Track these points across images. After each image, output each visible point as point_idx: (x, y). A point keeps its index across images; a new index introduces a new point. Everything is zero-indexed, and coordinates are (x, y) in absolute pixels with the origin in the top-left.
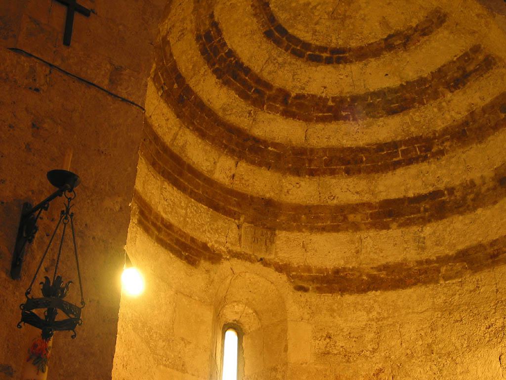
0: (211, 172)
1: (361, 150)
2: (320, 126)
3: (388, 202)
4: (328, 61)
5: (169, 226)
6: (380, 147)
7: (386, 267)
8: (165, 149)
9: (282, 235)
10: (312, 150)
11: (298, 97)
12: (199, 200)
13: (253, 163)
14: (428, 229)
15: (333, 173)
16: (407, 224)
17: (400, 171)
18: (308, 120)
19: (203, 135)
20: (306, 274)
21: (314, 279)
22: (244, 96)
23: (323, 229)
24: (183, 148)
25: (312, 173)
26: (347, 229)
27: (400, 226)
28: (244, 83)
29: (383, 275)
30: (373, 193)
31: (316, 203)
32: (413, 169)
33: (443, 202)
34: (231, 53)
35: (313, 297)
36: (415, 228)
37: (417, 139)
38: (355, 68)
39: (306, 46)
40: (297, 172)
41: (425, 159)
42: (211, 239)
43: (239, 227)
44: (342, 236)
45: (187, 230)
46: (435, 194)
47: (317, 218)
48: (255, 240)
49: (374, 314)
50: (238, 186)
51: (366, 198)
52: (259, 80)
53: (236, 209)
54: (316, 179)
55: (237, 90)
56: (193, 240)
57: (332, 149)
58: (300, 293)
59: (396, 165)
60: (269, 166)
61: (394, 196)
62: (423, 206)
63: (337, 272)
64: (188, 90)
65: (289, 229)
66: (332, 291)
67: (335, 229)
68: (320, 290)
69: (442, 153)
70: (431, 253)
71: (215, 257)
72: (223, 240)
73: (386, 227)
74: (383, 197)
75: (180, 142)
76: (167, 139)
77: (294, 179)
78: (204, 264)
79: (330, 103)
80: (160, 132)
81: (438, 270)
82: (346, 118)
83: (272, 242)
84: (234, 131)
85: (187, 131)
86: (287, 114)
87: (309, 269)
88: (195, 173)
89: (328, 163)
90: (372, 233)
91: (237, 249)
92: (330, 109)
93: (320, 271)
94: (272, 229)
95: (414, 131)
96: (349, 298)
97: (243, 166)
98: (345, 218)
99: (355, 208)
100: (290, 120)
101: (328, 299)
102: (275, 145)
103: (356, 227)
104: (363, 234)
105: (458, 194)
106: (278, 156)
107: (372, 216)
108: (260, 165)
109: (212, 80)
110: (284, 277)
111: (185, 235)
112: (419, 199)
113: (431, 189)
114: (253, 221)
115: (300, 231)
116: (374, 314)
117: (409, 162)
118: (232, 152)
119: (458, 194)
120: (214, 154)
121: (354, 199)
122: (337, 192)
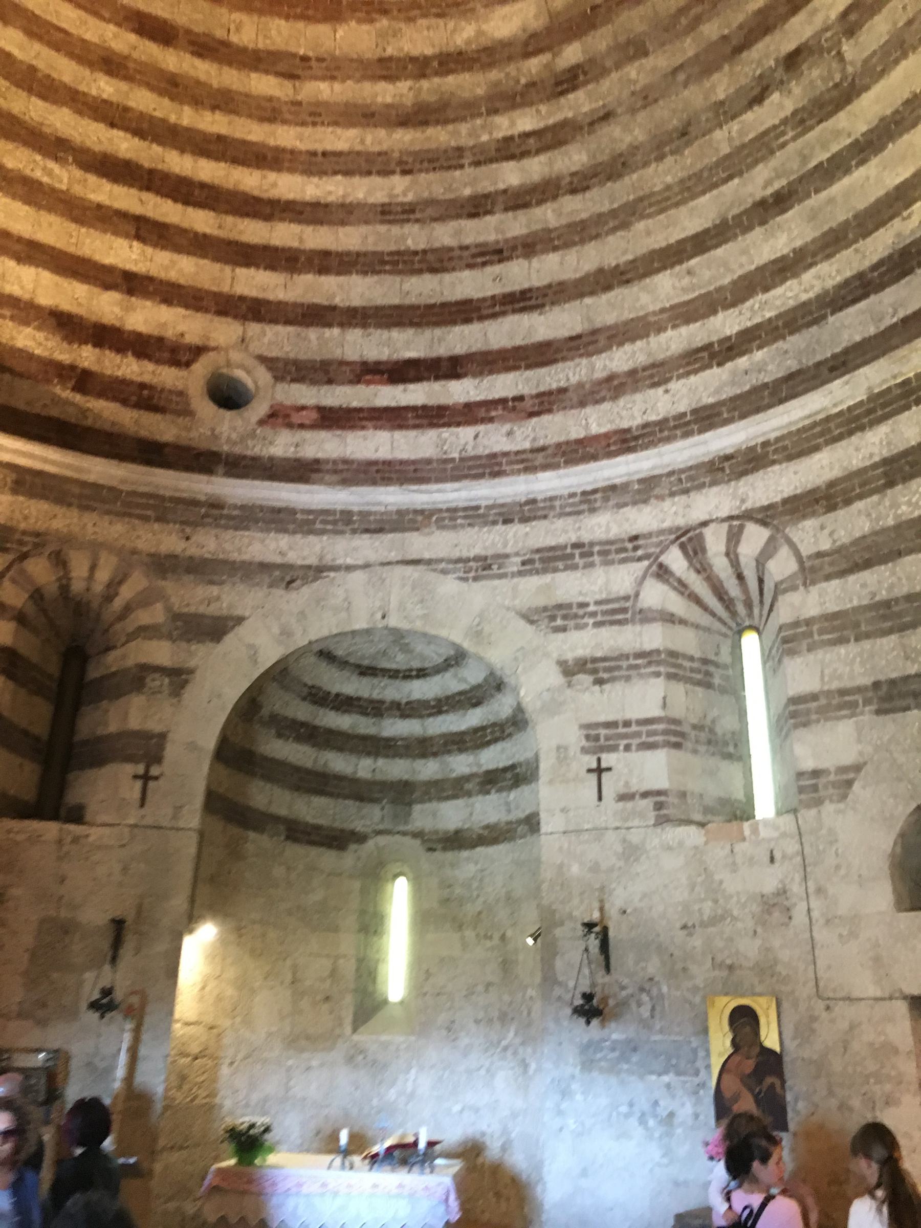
0: (355, 772)
1: (463, 733)
2: (431, 719)
3: (488, 772)
4: (418, 677)
5: (317, 828)
6: (476, 730)
7: (487, 827)
8: (308, 772)
9: (417, 808)
10: (431, 738)
11: (407, 703)
12: (346, 797)
13: (387, 756)
14: (513, 795)
15: (449, 752)
16: (500, 790)
17: (492, 747)
18: (421, 717)
19: (340, 749)
20: (434, 837)
21: (439, 841)
22: (364, 713)
23: (448, 798)
24: (325, 764)
25: (435, 755)
26: (463, 796)
27: (497, 791)
28: (360, 706)
29: (486, 833)
30: (480, 766)
31: (439, 776)
32: (499, 746)
33: (518, 774)
34: (337, 695)
35: (438, 855)
36: (504, 794)
37: (494, 725)
38: (437, 679)
39: (397, 672)
40: (424, 755)
41: (504, 739)
42: (359, 826)
43: (383, 809)
44: (460, 802)
45: (337, 825)
46: (513, 767)
47: (443, 790)
48: (395, 817)
49: (479, 866)
50: (379, 777)
51: (475, 769)
52: (372, 701)
53: (376, 795)
54: (438, 759)
55: (357, 713)
56: (342, 831)
57: (443, 735)
58: (430, 853)
59: (488, 743)
60: (401, 756)
61: (491, 766)
62: (509, 775)
63: (457, 832)
64: (315, 728)
65: (422, 801)
66: (453, 849)
67: (455, 797)
68: (445, 849)
69: (510, 735)
70: (513, 817)
71: (360, 838)
72: (369, 823)
73: (488, 793)
74: (484, 768)
75: (321, 762)
76: (309, 764)
77: (423, 761)
78: (353, 847)
79: (432, 703)
80: (299, 763)
81: (516, 831)
82: (447, 712)
83: (409, 814)
84: (365, 738)
85: (326, 752)
86: (404, 716)
87: (436, 832)
88: (340, 778)
89: (445, 744)
90: (480, 797)
91: (381, 827)
92: (433, 707)
93: (446, 832)
94: (410, 804)
95: (492, 719)
96: (465, 854)
97: (381, 762)
98: (462, 788)
99: (467, 778)
100: (407, 720)
101: (450, 855)
102: (402, 739)
103: (469, 794)
104: (473, 800)
105: (524, 769)
106: (407, 747)
107: (479, 784)
108: (394, 756)
109: (332, 714)
110: (418, 842)
111: (332, 829)
112: (505, 770)
113: (510, 763)
114: (393, 802)
115: (430, 800)
116: (479, 866)
117: (496, 740)
118: (369, 754)
119: (524, 769)
120: (353, 759)
121: (466, 771)
122: (454, 766)
